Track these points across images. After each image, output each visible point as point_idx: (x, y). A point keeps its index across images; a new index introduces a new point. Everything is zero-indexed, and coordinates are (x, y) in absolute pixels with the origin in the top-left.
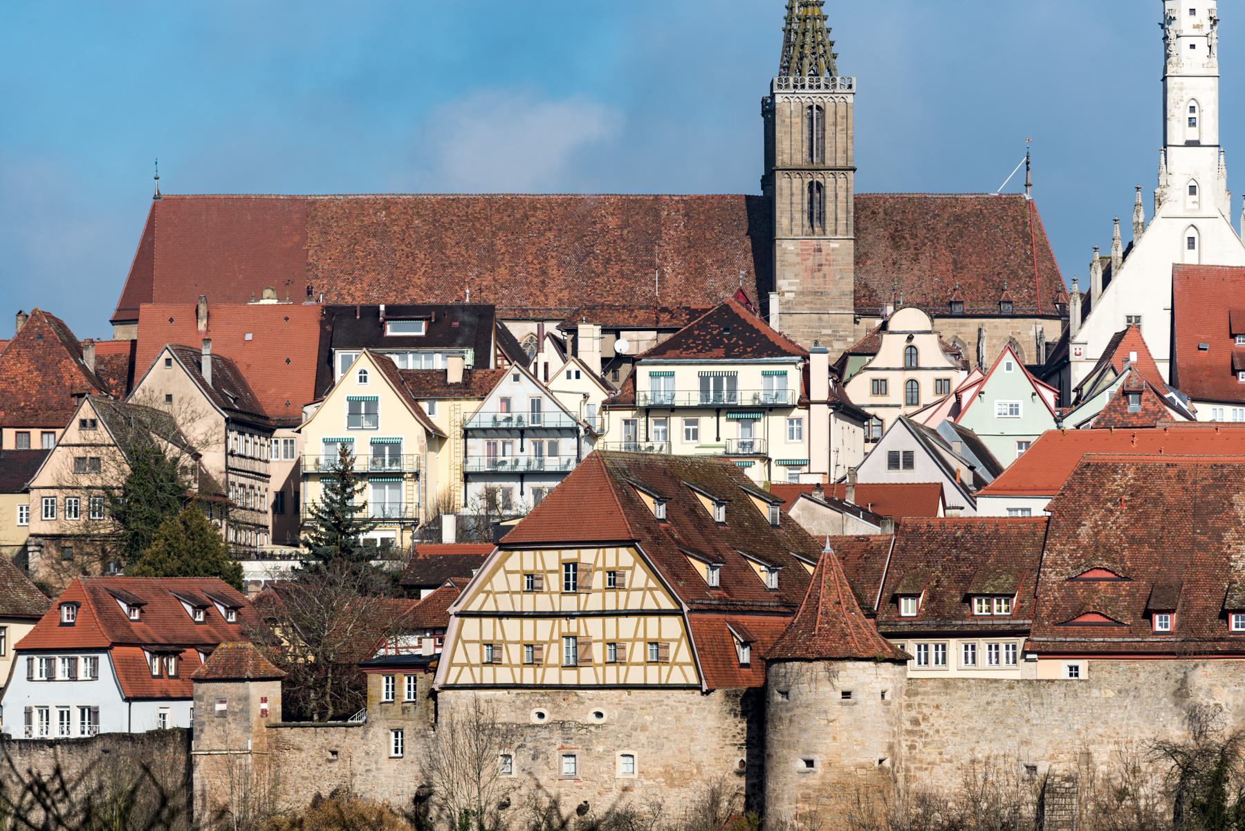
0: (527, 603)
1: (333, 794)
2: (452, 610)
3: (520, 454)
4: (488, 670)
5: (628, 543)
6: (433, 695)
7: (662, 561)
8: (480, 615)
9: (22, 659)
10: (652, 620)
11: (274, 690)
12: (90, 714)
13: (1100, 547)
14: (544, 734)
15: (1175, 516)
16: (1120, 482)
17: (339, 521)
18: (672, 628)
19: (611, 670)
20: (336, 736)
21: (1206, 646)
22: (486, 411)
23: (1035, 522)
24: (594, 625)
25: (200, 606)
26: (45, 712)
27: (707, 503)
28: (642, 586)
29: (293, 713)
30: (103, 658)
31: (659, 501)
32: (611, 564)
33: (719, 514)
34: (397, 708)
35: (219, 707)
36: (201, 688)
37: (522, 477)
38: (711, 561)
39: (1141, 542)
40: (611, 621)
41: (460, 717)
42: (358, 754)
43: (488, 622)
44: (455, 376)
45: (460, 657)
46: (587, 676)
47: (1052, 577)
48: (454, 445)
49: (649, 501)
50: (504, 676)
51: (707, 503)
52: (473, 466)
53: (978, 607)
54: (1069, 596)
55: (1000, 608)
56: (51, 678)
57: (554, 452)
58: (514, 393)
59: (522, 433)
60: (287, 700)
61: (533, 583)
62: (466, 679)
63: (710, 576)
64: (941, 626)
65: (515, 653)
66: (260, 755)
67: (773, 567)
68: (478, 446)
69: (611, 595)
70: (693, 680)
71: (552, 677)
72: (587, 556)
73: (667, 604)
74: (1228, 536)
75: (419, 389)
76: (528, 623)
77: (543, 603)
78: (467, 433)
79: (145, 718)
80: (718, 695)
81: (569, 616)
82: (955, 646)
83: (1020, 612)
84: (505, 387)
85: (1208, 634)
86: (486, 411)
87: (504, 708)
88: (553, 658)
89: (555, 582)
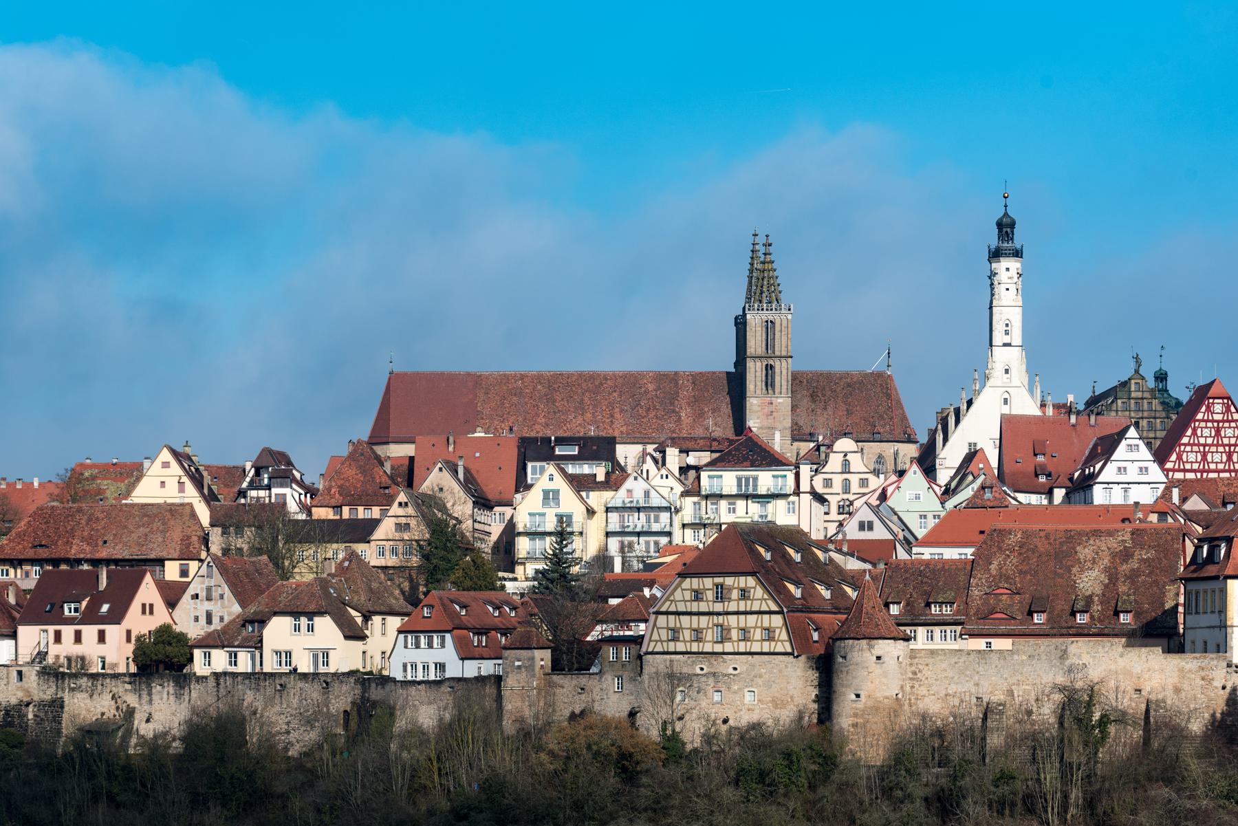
0: (694, 607)
1: (582, 712)
2: (651, 610)
3: (637, 522)
4: (672, 644)
5: (753, 574)
6: (640, 657)
7: (771, 584)
8: (667, 613)
9: (402, 636)
10: (766, 617)
11: (547, 654)
12: (441, 667)
13: (1003, 576)
14: (704, 679)
15: (1044, 558)
16: (1013, 540)
17: (559, 560)
18: (777, 621)
19: (742, 644)
20: (583, 680)
21: (1064, 631)
22: (618, 498)
23: (965, 561)
24: (732, 620)
25: (497, 608)
26: (414, 666)
27: (791, 551)
28: (760, 597)
29: (557, 667)
30: (448, 636)
31: (767, 550)
32: (742, 585)
33: (797, 557)
34: (619, 664)
35: (517, 663)
36: (507, 653)
37: (639, 534)
38: (797, 583)
39: (1026, 573)
40: (742, 617)
41: (662, 668)
42: (596, 690)
43: (671, 617)
44: (601, 477)
45: (655, 637)
46: (728, 647)
47: (975, 592)
48: (600, 516)
49: (762, 550)
50: (681, 647)
51: (791, 551)
52: (611, 528)
53: (935, 610)
54: (986, 603)
55: (947, 610)
56: (418, 646)
57: (657, 520)
58: (634, 489)
59: (639, 509)
60: (553, 661)
61: (698, 595)
62: (659, 648)
63: (796, 592)
64: (914, 618)
65: (687, 635)
66: (539, 689)
67: (828, 586)
68: (614, 517)
69: (742, 603)
70: (789, 650)
71: (708, 648)
72: (729, 581)
73: (774, 608)
74: (1074, 570)
75: (581, 484)
76: (695, 618)
77: (703, 607)
78: (608, 510)
79: (471, 669)
80: (803, 658)
81: (718, 614)
82: (921, 631)
83: (958, 612)
84: (629, 484)
85: (1064, 624)
86: (618, 498)
87: (683, 665)
88: (709, 637)
89: (710, 595)
